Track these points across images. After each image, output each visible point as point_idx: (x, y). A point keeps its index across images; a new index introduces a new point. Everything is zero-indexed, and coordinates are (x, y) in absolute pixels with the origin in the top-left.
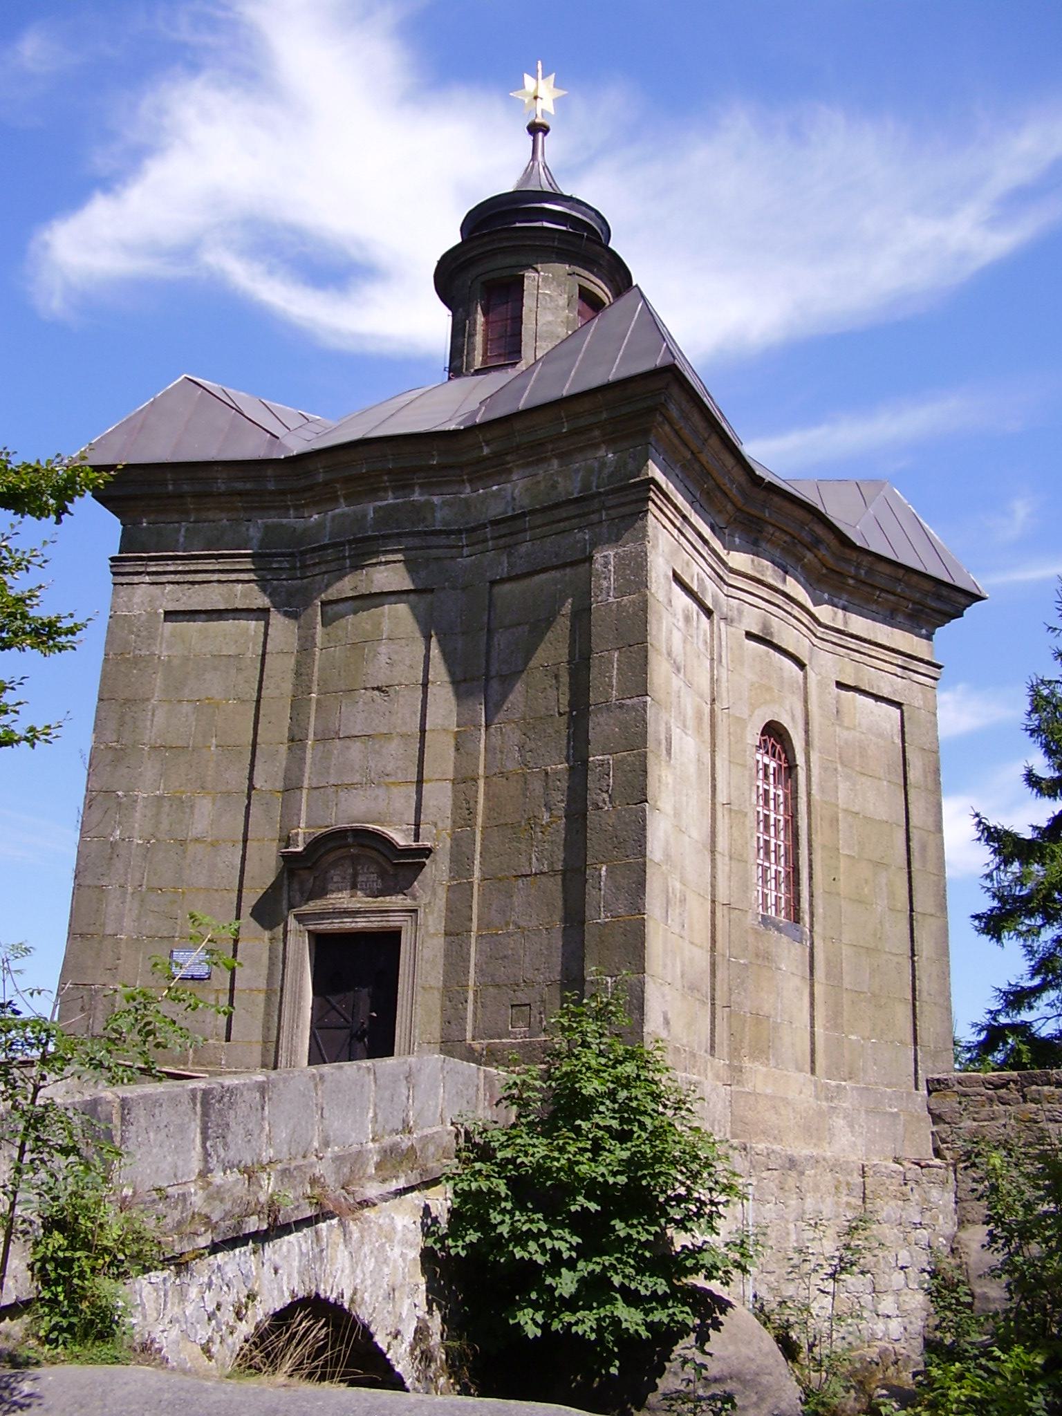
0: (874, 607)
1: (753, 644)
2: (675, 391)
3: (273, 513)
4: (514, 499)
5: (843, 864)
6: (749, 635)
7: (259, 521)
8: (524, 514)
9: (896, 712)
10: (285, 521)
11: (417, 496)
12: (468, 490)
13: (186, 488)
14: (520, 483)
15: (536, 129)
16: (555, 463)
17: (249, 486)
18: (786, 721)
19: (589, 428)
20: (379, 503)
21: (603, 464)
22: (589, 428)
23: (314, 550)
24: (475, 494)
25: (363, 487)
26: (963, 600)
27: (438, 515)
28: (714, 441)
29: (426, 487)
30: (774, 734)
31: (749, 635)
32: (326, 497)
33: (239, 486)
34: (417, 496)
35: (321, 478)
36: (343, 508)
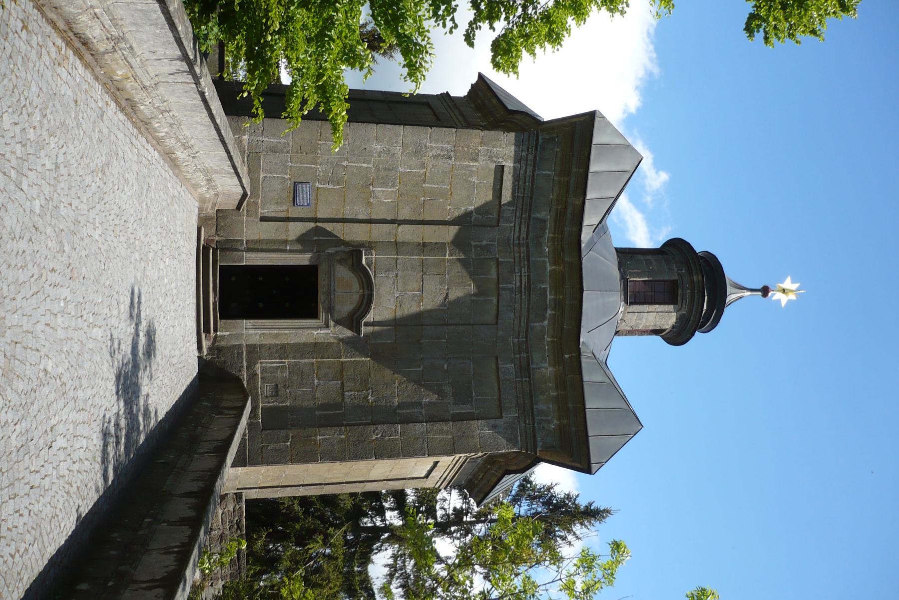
0: (476, 470)
3: (553, 224)
4: (539, 368)
7: (549, 217)
8: (529, 377)
10: (547, 231)
12: (549, 340)
13: (573, 180)
15: (765, 291)
17: (569, 216)
20: (548, 289)
21: (549, 422)
23: (528, 252)
24: (546, 343)
25: (559, 282)
26: (479, 499)
27: (537, 324)
33: (569, 210)
34: (549, 311)
36: (549, 268)
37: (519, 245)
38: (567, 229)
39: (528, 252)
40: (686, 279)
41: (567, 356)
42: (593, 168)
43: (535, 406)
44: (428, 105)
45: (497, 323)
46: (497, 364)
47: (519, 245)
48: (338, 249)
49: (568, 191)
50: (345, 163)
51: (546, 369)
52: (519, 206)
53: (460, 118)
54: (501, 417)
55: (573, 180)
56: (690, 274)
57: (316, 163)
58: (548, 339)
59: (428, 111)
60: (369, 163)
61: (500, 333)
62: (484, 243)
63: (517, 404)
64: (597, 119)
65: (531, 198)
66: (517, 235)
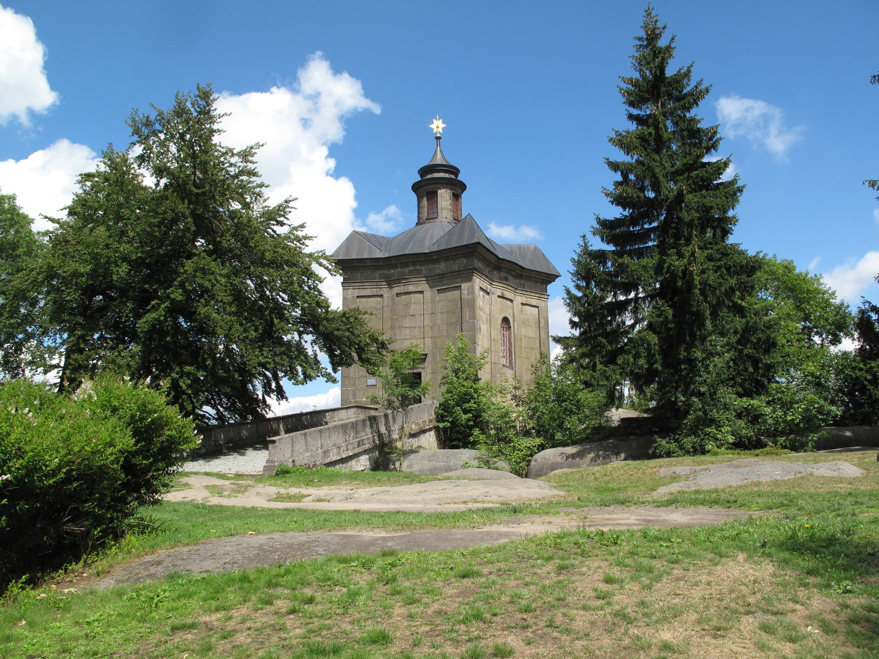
1: (500, 299)
2: (479, 246)
5: (523, 349)
6: (499, 296)
9: (537, 309)
11: (418, 267)
13: (359, 265)
15: (438, 138)
16: (452, 261)
17: (376, 264)
18: (508, 316)
28: (489, 253)
29: (420, 265)
30: (506, 320)
31: (499, 296)
32: (395, 267)
33: (373, 264)
35: (394, 262)
36: (399, 269)
38: (381, 264)
40: (426, 188)
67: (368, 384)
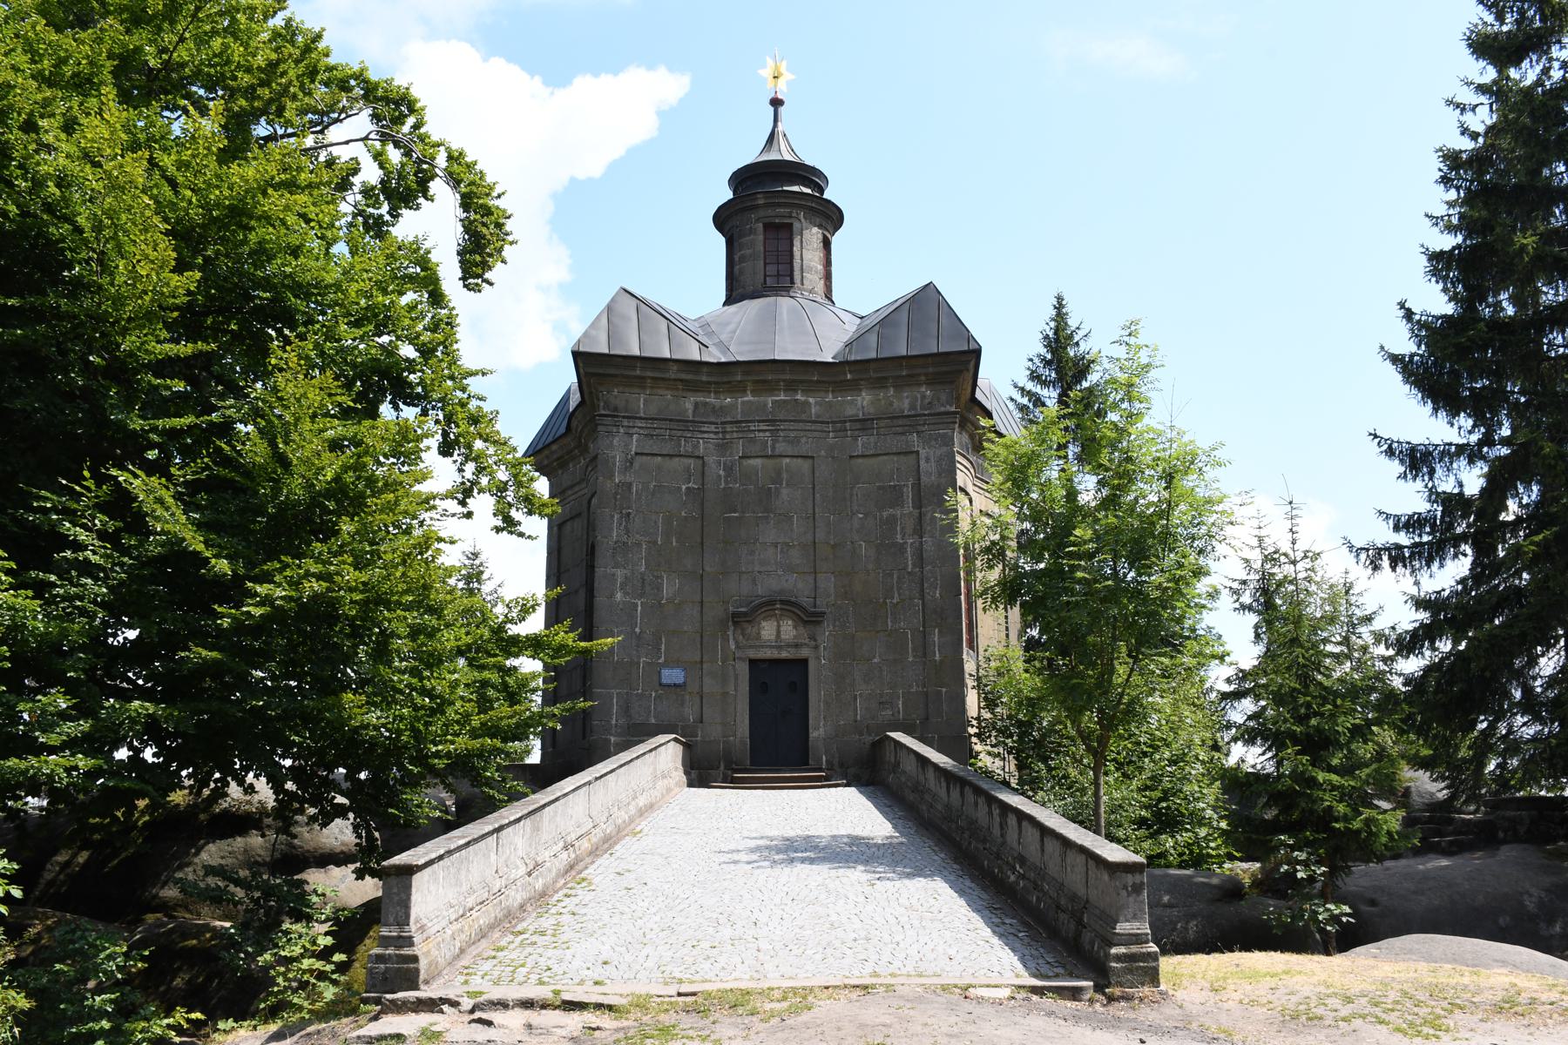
13: (649, 374)
14: (868, 398)
17: (689, 377)
19: (919, 375)
21: (924, 397)
22: (919, 375)
23: (731, 423)
25: (764, 387)
29: (805, 392)
33: (683, 376)
34: (799, 397)
35: (739, 378)
36: (749, 398)
37: (724, 432)
38: (704, 378)
39: (731, 423)
40: (762, 213)
41: (849, 376)
42: (637, 353)
43: (906, 413)
44: (561, 526)
45: (813, 457)
46: (858, 456)
47: (724, 432)
48: (731, 637)
49: (663, 379)
50: (637, 630)
51: (863, 401)
52: (679, 433)
53: (576, 489)
54: (917, 452)
55: (649, 374)
56: (757, 207)
57: (639, 663)
58: (830, 397)
59: (568, 527)
60: (636, 605)
61: (823, 453)
62: (721, 472)
63: (903, 434)
64: (581, 349)
65: (671, 420)
66: (712, 436)
67: (664, 681)
